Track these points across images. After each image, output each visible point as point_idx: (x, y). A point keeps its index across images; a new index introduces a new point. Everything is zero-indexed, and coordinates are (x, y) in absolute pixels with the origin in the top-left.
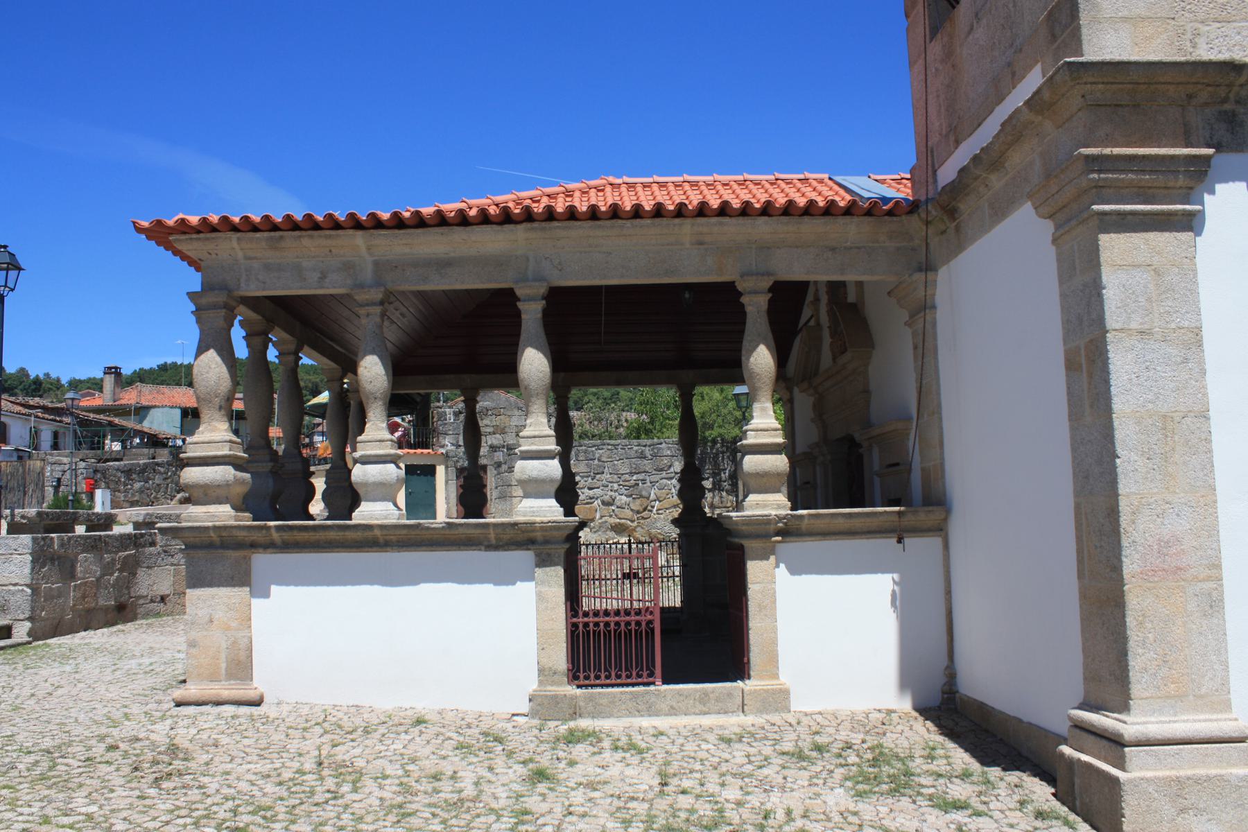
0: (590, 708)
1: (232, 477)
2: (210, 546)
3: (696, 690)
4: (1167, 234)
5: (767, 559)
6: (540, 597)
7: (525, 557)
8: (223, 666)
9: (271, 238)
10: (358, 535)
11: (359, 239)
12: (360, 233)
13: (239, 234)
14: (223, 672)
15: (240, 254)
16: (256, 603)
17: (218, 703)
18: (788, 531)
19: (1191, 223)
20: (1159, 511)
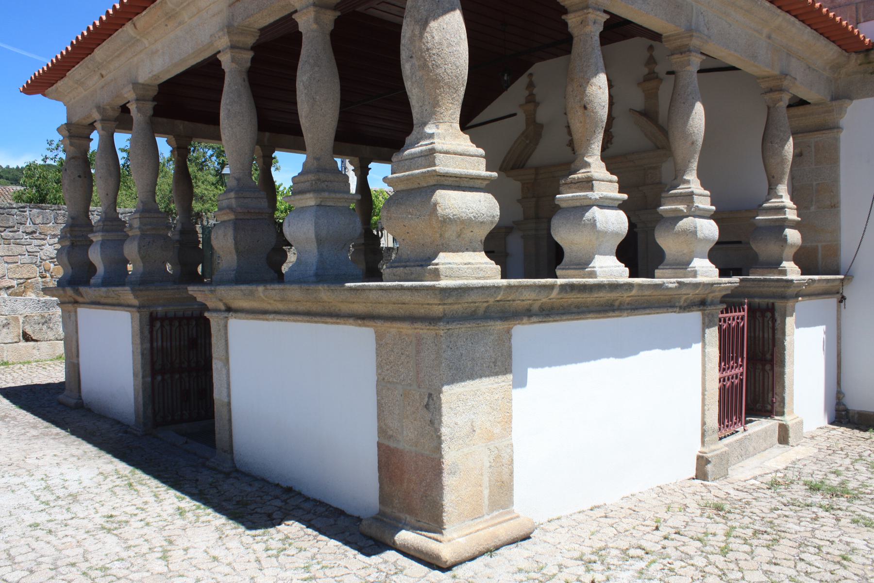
7: (695, 317)
8: (486, 492)
10: (604, 296)
14: (486, 501)
16: (517, 393)
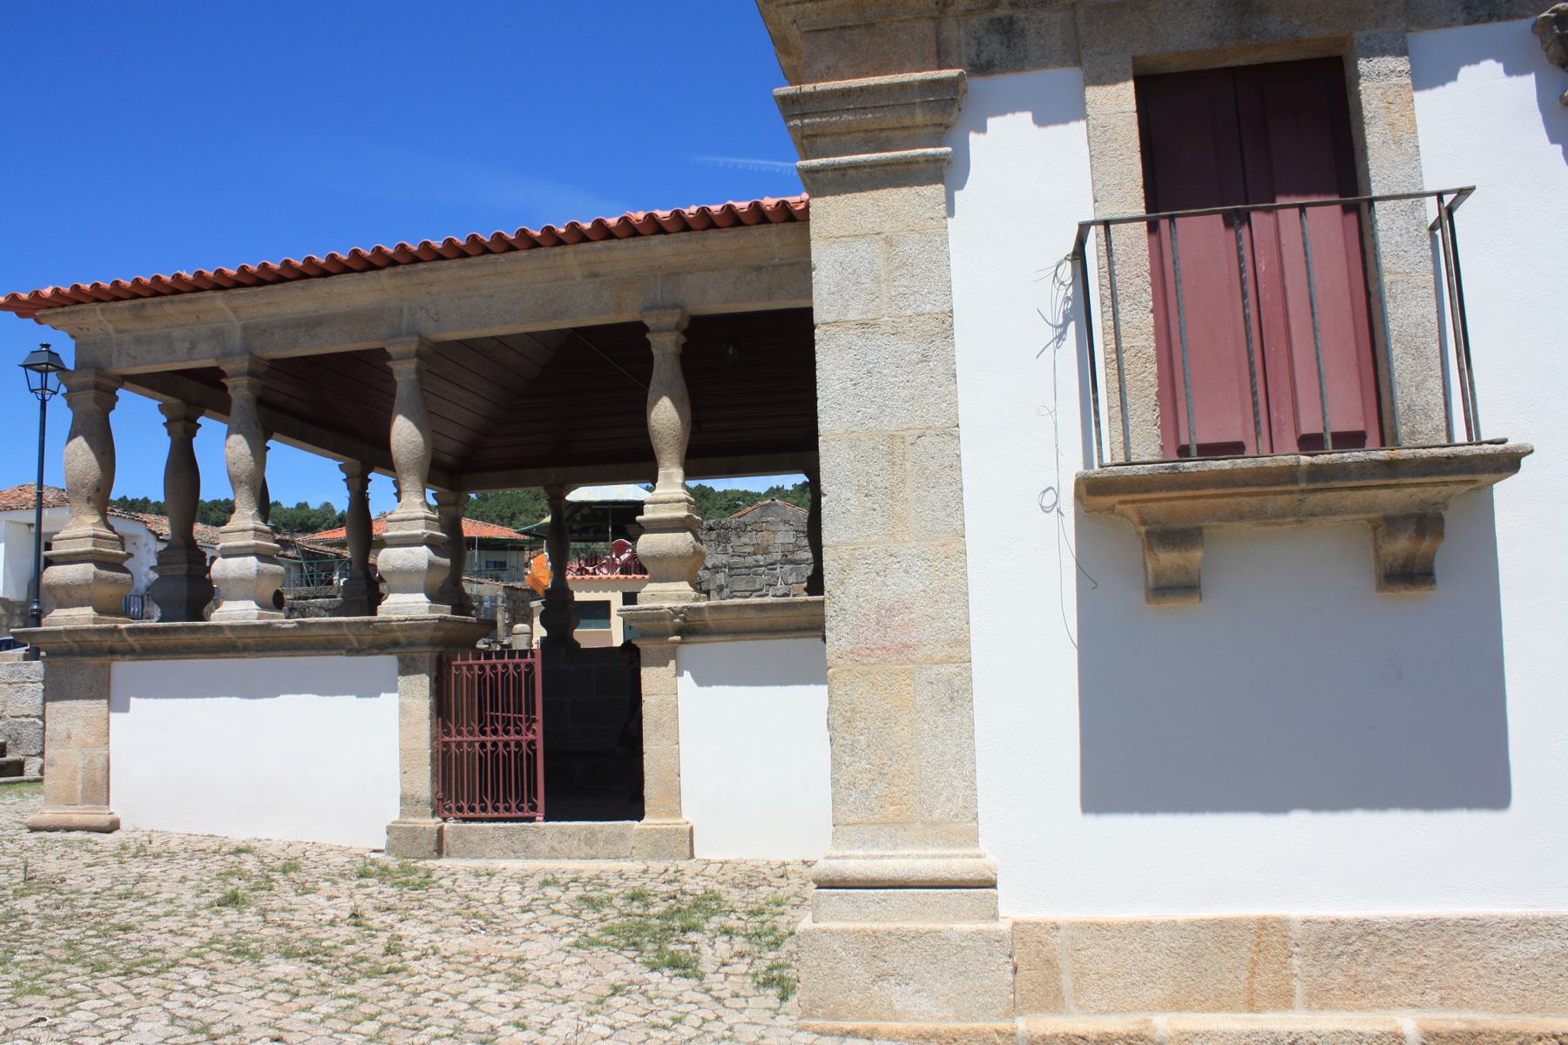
0: (459, 845)
1: (91, 576)
2: (70, 653)
3: (581, 829)
4: (905, 190)
5: (666, 665)
6: (403, 710)
7: (389, 662)
8: (80, 787)
9: (134, 307)
10: (210, 638)
11: (218, 300)
12: (219, 294)
13: (102, 305)
15: (110, 328)
17: (69, 829)
18: (691, 627)
19: (945, 173)
20: (879, 566)
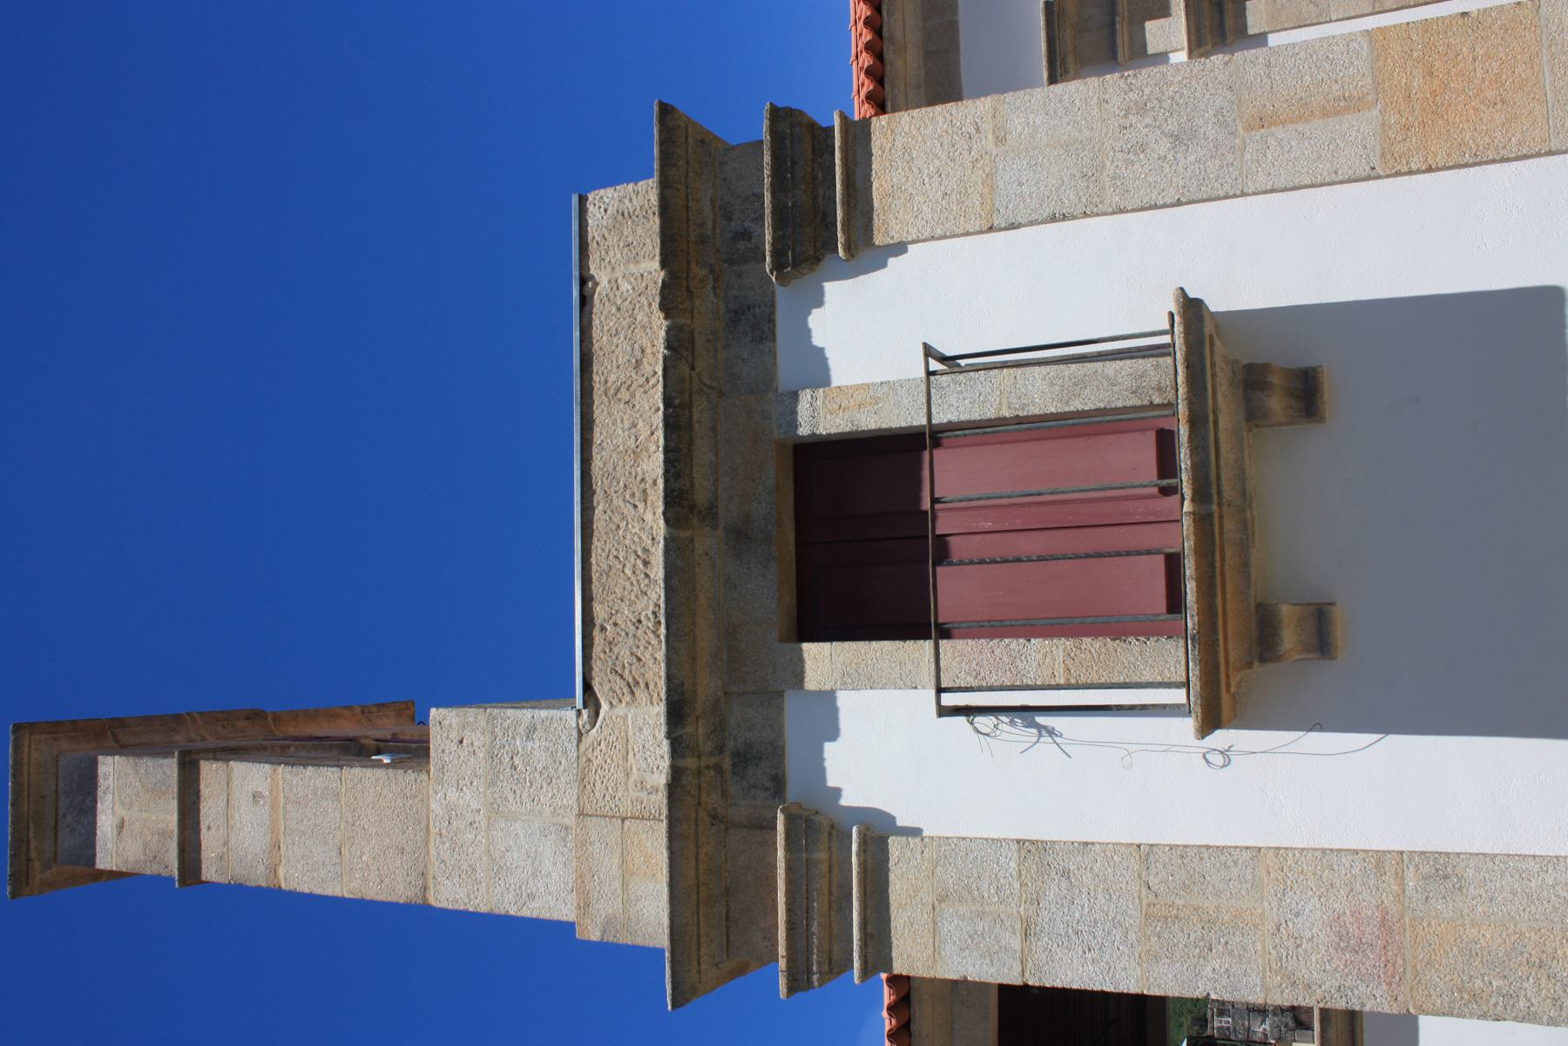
4: (892, 877)
19: (878, 832)
20: (1290, 943)
